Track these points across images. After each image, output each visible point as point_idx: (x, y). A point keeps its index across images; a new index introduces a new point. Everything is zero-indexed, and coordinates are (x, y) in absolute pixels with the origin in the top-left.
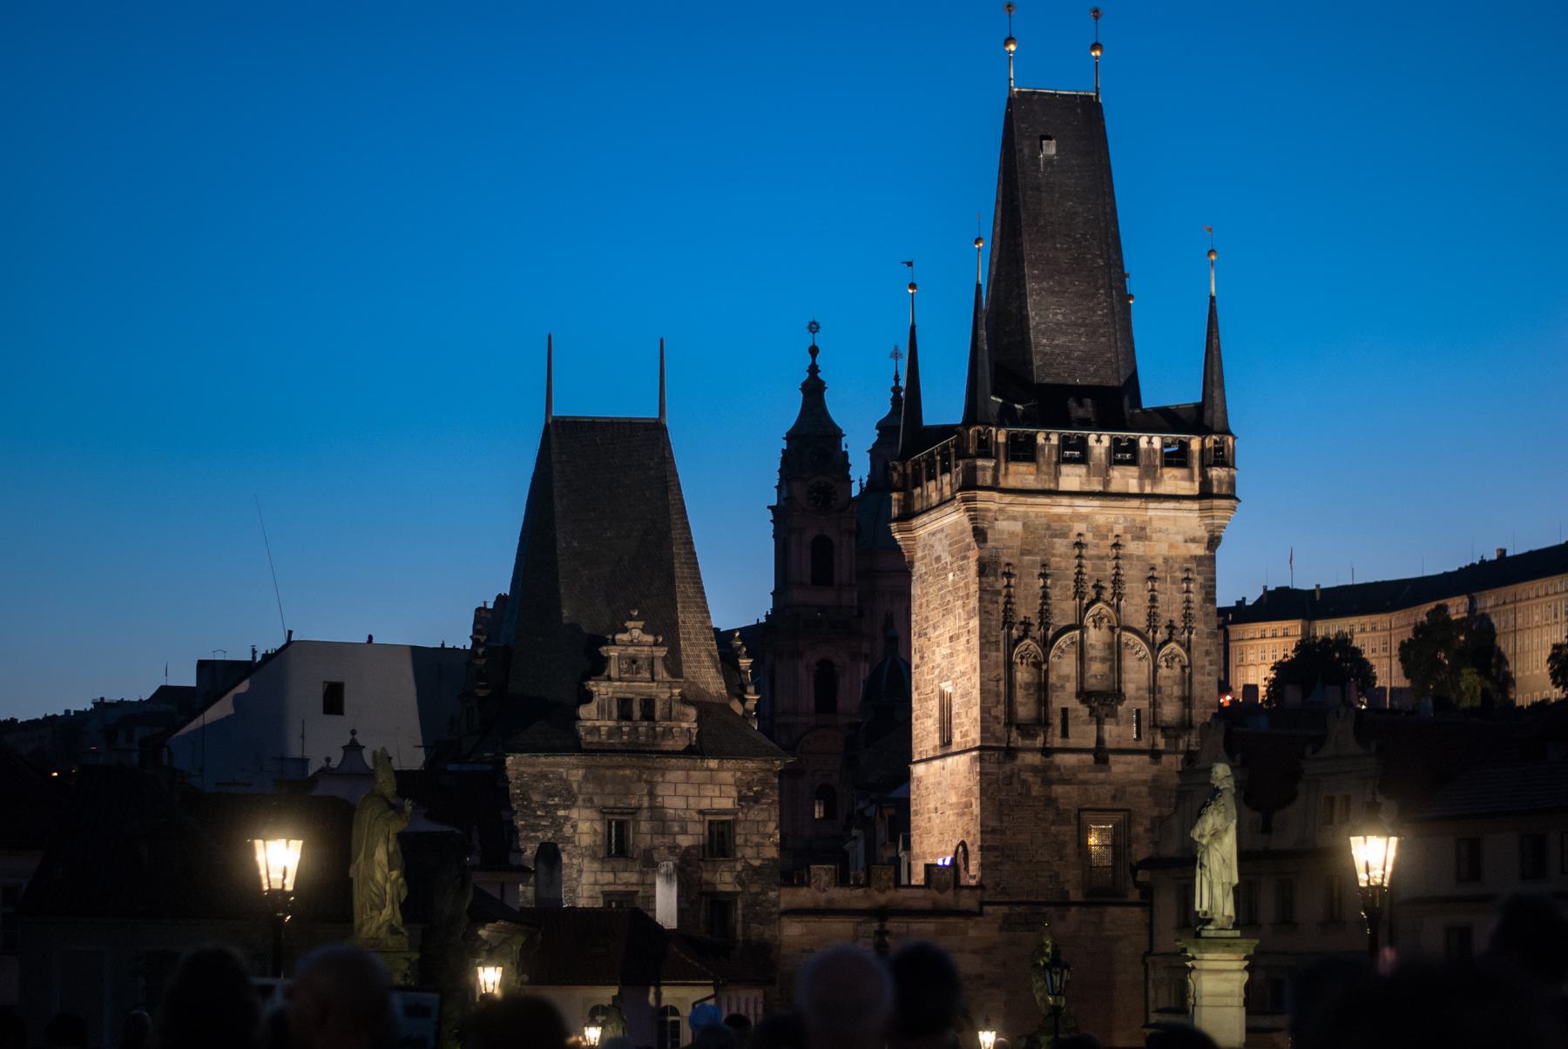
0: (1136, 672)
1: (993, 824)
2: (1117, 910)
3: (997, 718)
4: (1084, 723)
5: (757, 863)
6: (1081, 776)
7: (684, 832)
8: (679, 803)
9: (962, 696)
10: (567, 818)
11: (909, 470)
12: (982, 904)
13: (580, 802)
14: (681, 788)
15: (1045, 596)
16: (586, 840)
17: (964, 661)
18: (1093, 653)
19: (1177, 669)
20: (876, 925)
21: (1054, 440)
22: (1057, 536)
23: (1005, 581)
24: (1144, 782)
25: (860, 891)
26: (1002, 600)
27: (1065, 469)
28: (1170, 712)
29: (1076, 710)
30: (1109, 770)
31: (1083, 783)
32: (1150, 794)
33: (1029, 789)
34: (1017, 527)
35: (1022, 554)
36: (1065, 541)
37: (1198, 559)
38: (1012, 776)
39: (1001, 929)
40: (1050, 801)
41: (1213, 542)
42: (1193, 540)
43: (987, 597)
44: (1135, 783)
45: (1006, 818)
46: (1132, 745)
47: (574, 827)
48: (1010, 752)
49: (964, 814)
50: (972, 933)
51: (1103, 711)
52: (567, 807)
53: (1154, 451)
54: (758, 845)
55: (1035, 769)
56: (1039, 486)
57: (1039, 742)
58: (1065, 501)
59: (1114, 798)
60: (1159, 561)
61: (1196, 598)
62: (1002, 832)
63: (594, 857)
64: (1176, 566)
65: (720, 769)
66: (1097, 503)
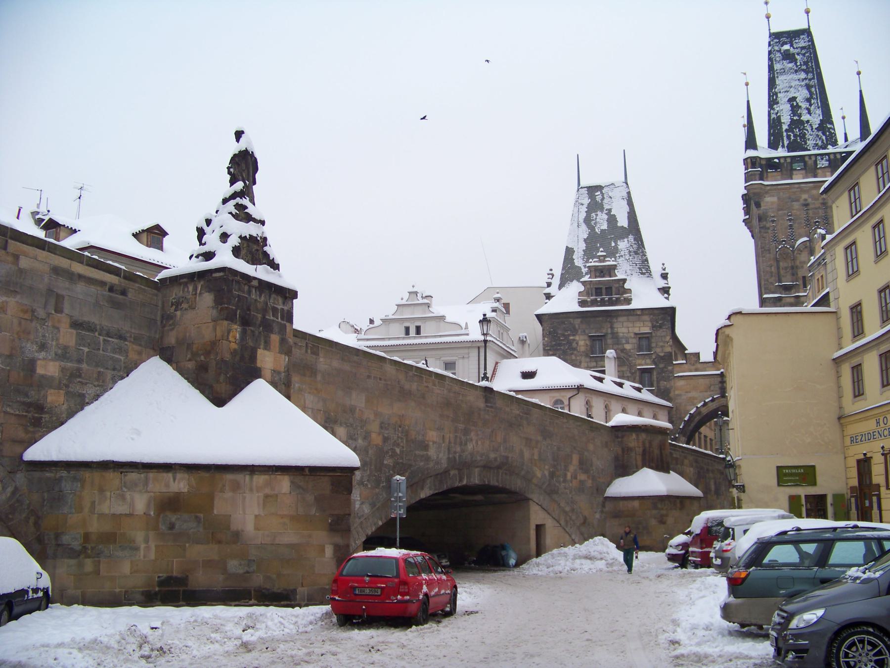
5: (662, 354)
7: (628, 343)
8: (625, 330)
10: (574, 340)
13: (579, 332)
14: (625, 324)
16: (583, 349)
27: (794, 172)
34: (775, 199)
35: (779, 210)
47: (577, 343)
52: (574, 335)
54: (662, 347)
63: (587, 356)
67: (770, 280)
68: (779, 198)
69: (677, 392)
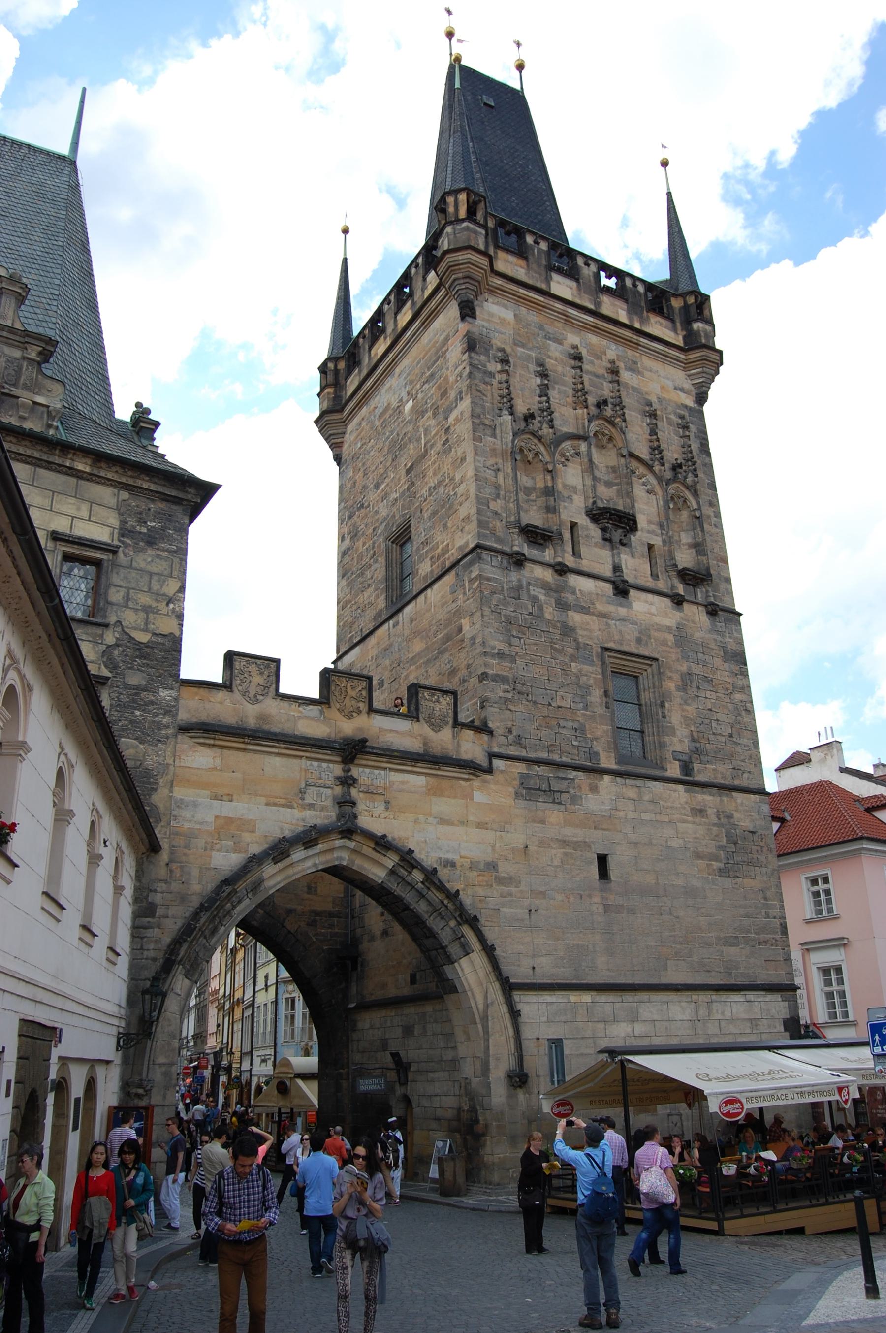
0: (647, 508)
1: (499, 645)
2: (658, 786)
3: (496, 513)
4: (596, 545)
6: (600, 607)
9: (434, 513)
11: (342, 365)
12: (492, 756)
15: (544, 391)
17: (435, 474)
18: (597, 473)
19: (685, 515)
20: (338, 770)
21: (544, 246)
22: (550, 339)
23: (499, 367)
24: (669, 629)
25: (314, 710)
26: (495, 382)
27: (556, 277)
28: (685, 558)
29: (587, 529)
30: (629, 606)
31: (603, 615)
32: (677, 646)
33: (541, 608)
35: (515, 344)
36: (560, 347)
37: (690, 409)
38: (519, 587)
39: (517, 795)
40: (568, 631)
41: (702, 398)
42: (682, 390)
43: (479, 375)
44: (659, 628)
45: (515, 641)
46: (650, 583)
48: (519, 561)
49: (441, 653)
50: (478, 796)
51: (617, 535)
53: (638, 292)
55: (545, 586)
56: (530, 282)
57: (548, 555)
58: (559, 306)
59: (639, 641)
60: (654, 399)
61: (695, 446)
62: (514, 661)
64: (670, 409)
65: (91, 478)
66: (592, 319)
67: (492, 505)
68: (515, 315)
69: (179, 793)
